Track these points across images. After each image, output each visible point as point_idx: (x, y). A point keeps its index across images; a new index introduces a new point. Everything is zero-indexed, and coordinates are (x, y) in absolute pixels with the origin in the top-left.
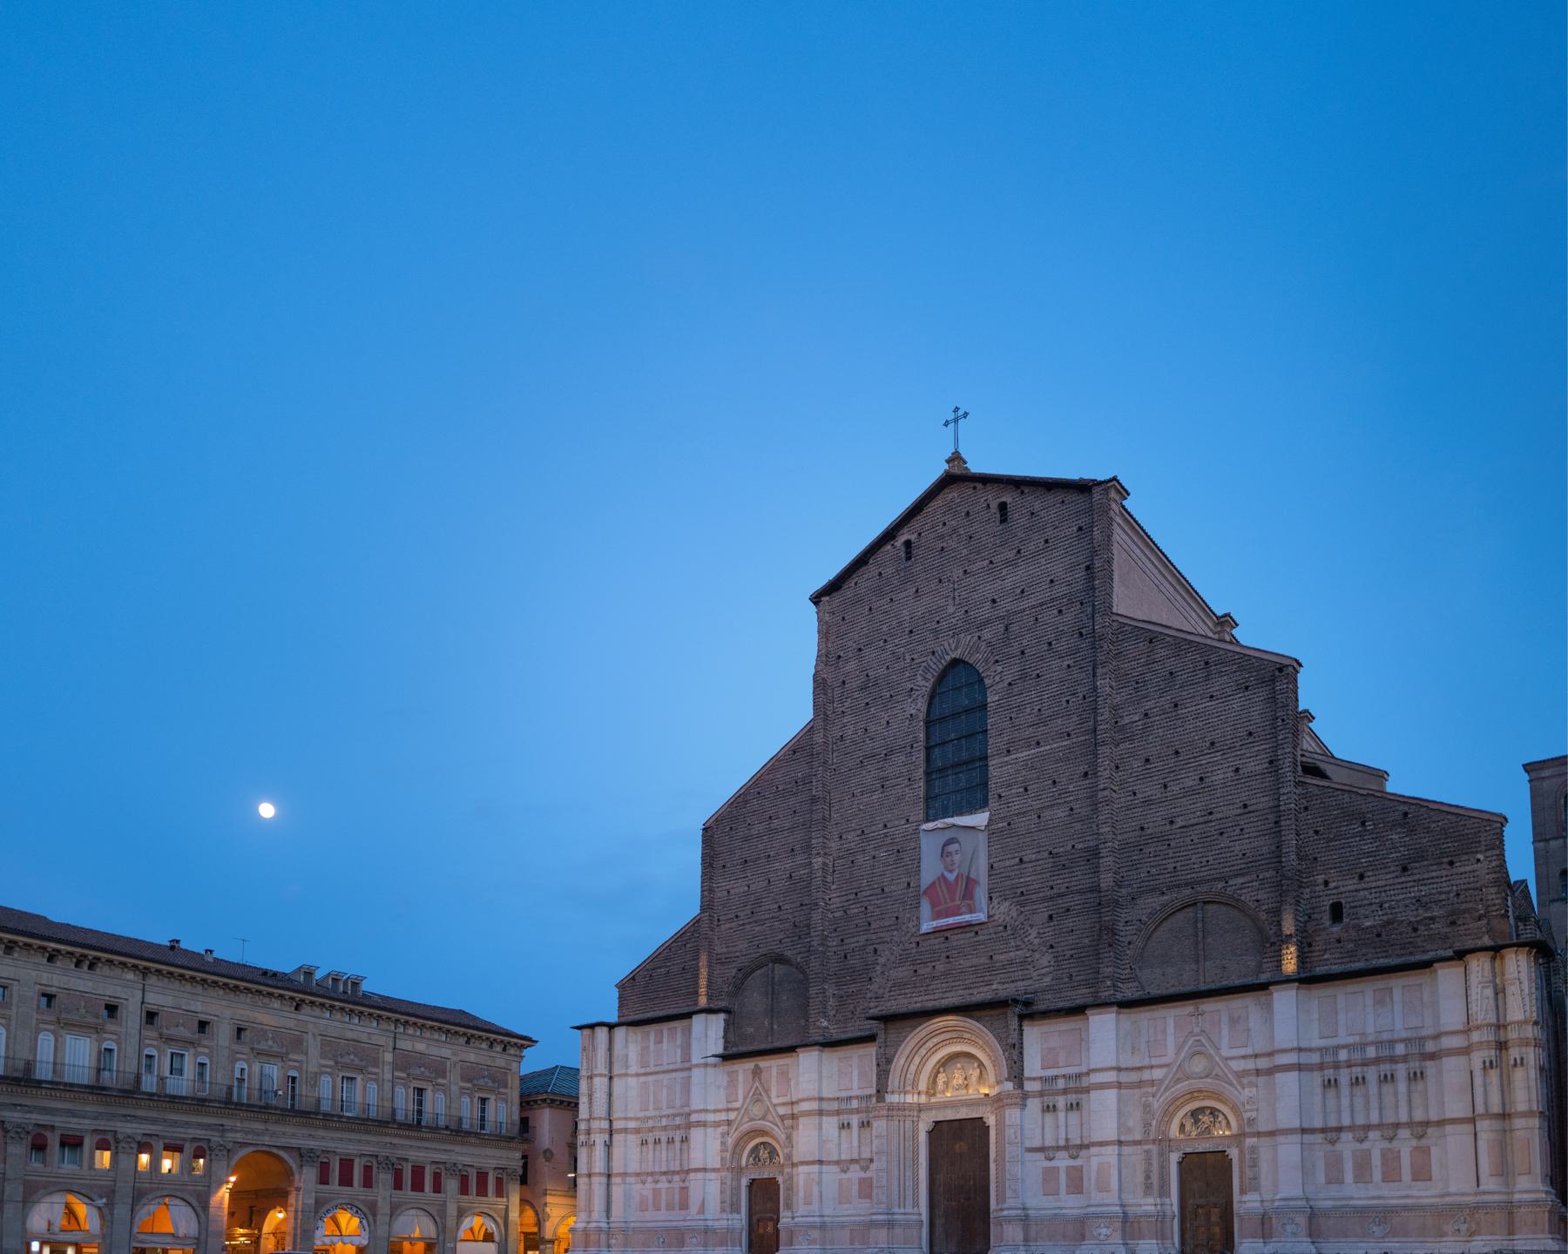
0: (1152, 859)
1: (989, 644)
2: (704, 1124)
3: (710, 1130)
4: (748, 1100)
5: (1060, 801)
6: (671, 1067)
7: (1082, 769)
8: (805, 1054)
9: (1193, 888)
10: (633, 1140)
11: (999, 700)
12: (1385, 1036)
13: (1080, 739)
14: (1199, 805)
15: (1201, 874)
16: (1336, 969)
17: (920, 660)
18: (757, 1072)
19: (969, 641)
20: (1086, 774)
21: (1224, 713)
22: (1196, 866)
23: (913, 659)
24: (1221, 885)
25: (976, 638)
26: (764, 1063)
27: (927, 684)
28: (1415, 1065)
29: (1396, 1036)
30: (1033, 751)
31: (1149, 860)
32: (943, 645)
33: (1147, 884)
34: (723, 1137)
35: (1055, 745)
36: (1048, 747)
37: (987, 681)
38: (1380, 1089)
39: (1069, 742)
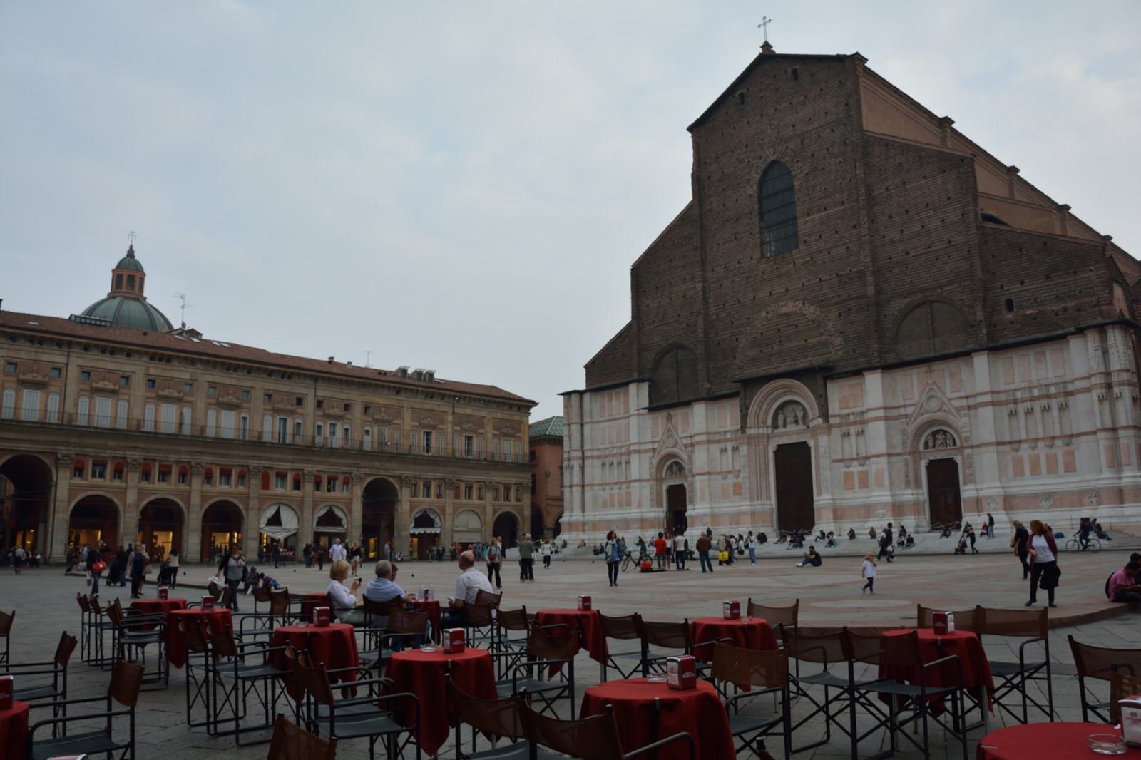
1: (793, 151)
2: (639, 452)
3: (643, 455)
7: (852, 224)
10: (598, 463)
12: (1043, 382)
16: (1011, 341)
18: (669, 418)
20: (855, 226)
24: (939, 291)
26: (673, 412)
28: (1062, 400)
29: (1050, 382)
34: (650, 458)
37: (793, 173)
38: (1043, 415)
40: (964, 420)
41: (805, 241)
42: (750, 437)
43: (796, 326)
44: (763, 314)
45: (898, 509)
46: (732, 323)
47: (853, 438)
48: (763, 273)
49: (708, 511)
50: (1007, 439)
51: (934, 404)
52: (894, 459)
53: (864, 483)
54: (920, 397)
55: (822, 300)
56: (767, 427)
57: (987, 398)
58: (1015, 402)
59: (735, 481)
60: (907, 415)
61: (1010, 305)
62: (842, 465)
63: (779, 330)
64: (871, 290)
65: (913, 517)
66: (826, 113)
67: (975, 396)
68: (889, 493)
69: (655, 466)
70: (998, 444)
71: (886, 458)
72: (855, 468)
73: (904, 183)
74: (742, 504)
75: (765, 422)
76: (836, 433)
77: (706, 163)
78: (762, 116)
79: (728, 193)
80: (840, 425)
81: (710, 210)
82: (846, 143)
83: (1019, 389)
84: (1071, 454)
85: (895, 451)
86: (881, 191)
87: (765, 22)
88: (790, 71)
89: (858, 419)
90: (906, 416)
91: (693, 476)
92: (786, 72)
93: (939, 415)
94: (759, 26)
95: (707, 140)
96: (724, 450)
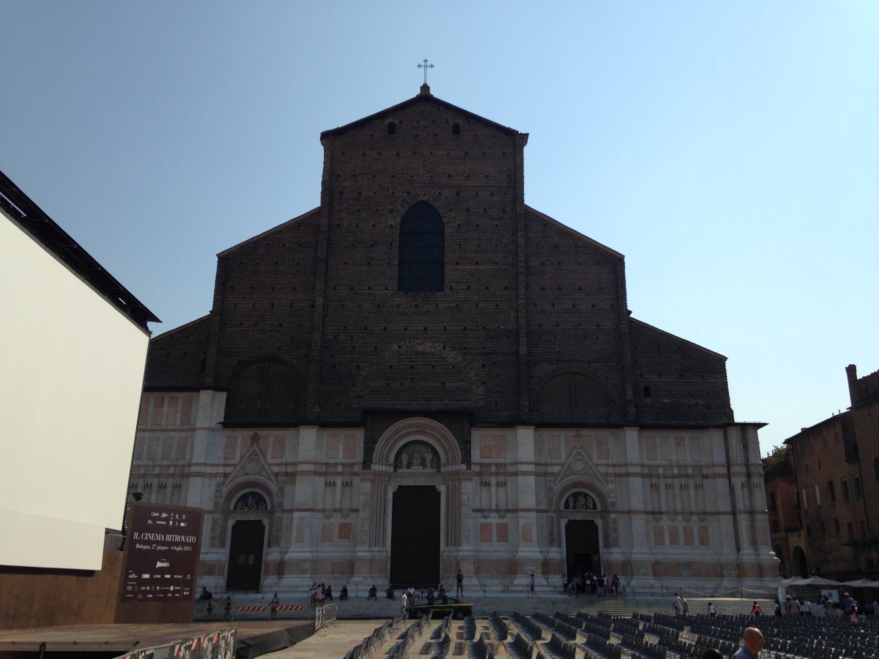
0: (546, 343)
4: (245, 459)
5: (490, 299)
6: (170, 427)
8: (306, 430)
9: (570, 364)
11: (452, 232)
13: (503, 267)
14: (573, 319)
15: (574, 357)
17: (399, 195)
18: (255, 439)
19: (433, 194)
20: (506, 288)
21: (586, 274)
22: (572, 352)
23: (393, 193)
24: (587, 365)
25: (438, 193)
26: (262, 433)
27: (404, 210)
30: (474, 267)
31: (544, 343)
32: (416, 191)
33: (543, 356)
35: (488, 267)
36: (483, 267)
37: (444, 219)
39: (496, 267)
40: (611, 486)
41: (451, 288)
42: (377, 474)
43: (433, 367)
44: (395, 347)
45: (546, 567)
46: (354, 348)
47: (493, 489)
48: (398, 306)
49: (308, 555)
50: (649, 509)
51: (579, 466)
52: (539, 514)
53: (503, 536)
54: (567, 458)
55: (465, 348)
56: (390, 465)
57: (637, 470)
58: (658, 476)
59: (343, 521)
60: (553, 473)
61: (647, 392)
62: (480, 515)
63: (412, 367)
64: (523, 350)
65: (558, 576)
66: (487, 176)
67: (621, 466)
68: (538, 550)
69: (224, 495)
70: (647, 513)
71: (535, 513)
72: (494, 520)
73: (560, 263)
74: (358, 548)
75: (387, 460)
76: (476, 480)
77: (339, 176)
78: (414, 153)
79: (363, 215)
80: (480, 474)
81: (338, 225)
82: (504, 210)
83: (660, 466)
84: (705, 529)
85: (539, 508)
86: (537, 264)
87: (426, 65)
88: (451, 123)
89: (501, 471)
90: (553, 474)
91: (283, 511)
92: (447, 122)
93: (584, 479)
94: (419, 66)
95: (343, 153)
96: (331, 485)
